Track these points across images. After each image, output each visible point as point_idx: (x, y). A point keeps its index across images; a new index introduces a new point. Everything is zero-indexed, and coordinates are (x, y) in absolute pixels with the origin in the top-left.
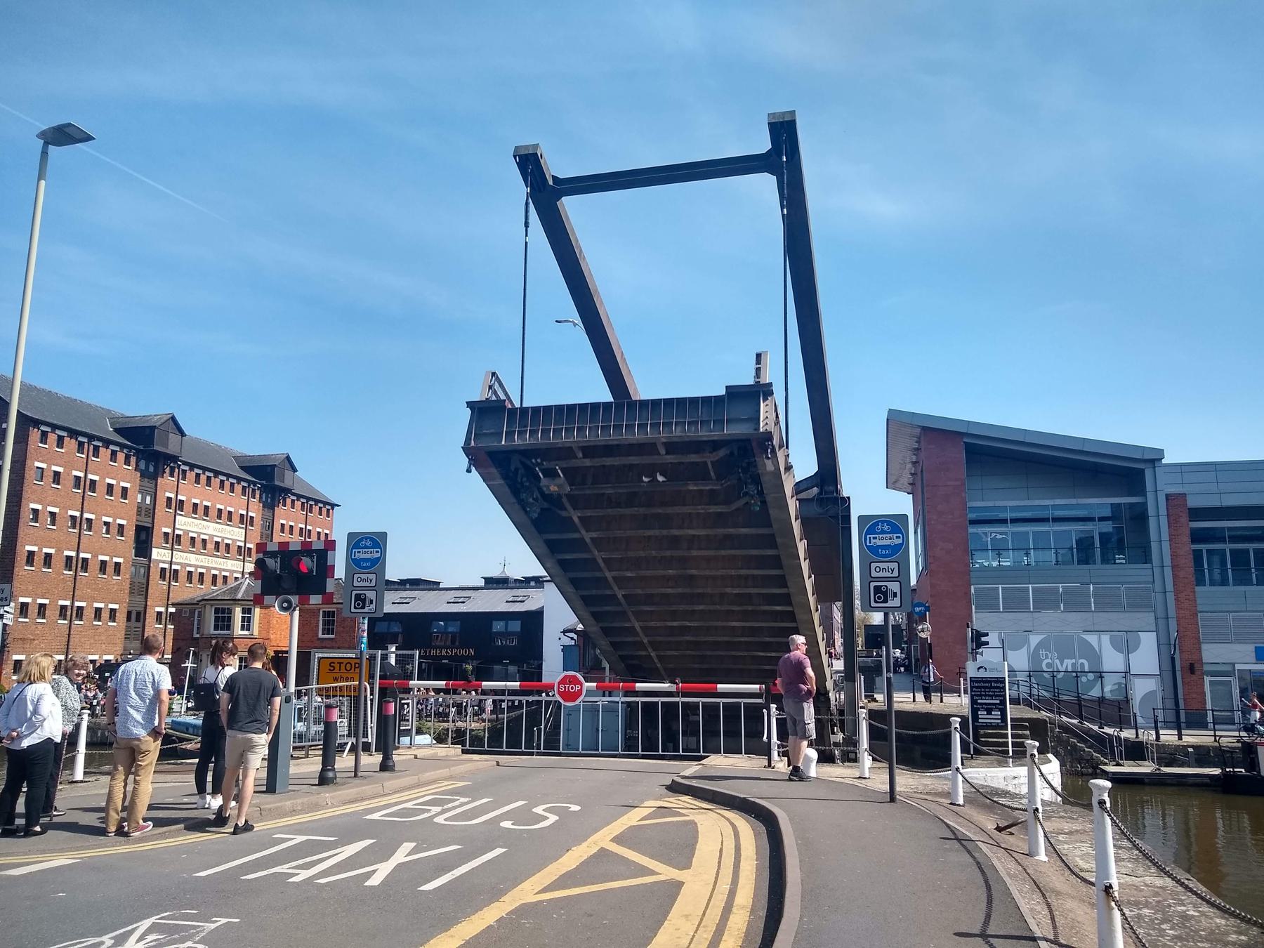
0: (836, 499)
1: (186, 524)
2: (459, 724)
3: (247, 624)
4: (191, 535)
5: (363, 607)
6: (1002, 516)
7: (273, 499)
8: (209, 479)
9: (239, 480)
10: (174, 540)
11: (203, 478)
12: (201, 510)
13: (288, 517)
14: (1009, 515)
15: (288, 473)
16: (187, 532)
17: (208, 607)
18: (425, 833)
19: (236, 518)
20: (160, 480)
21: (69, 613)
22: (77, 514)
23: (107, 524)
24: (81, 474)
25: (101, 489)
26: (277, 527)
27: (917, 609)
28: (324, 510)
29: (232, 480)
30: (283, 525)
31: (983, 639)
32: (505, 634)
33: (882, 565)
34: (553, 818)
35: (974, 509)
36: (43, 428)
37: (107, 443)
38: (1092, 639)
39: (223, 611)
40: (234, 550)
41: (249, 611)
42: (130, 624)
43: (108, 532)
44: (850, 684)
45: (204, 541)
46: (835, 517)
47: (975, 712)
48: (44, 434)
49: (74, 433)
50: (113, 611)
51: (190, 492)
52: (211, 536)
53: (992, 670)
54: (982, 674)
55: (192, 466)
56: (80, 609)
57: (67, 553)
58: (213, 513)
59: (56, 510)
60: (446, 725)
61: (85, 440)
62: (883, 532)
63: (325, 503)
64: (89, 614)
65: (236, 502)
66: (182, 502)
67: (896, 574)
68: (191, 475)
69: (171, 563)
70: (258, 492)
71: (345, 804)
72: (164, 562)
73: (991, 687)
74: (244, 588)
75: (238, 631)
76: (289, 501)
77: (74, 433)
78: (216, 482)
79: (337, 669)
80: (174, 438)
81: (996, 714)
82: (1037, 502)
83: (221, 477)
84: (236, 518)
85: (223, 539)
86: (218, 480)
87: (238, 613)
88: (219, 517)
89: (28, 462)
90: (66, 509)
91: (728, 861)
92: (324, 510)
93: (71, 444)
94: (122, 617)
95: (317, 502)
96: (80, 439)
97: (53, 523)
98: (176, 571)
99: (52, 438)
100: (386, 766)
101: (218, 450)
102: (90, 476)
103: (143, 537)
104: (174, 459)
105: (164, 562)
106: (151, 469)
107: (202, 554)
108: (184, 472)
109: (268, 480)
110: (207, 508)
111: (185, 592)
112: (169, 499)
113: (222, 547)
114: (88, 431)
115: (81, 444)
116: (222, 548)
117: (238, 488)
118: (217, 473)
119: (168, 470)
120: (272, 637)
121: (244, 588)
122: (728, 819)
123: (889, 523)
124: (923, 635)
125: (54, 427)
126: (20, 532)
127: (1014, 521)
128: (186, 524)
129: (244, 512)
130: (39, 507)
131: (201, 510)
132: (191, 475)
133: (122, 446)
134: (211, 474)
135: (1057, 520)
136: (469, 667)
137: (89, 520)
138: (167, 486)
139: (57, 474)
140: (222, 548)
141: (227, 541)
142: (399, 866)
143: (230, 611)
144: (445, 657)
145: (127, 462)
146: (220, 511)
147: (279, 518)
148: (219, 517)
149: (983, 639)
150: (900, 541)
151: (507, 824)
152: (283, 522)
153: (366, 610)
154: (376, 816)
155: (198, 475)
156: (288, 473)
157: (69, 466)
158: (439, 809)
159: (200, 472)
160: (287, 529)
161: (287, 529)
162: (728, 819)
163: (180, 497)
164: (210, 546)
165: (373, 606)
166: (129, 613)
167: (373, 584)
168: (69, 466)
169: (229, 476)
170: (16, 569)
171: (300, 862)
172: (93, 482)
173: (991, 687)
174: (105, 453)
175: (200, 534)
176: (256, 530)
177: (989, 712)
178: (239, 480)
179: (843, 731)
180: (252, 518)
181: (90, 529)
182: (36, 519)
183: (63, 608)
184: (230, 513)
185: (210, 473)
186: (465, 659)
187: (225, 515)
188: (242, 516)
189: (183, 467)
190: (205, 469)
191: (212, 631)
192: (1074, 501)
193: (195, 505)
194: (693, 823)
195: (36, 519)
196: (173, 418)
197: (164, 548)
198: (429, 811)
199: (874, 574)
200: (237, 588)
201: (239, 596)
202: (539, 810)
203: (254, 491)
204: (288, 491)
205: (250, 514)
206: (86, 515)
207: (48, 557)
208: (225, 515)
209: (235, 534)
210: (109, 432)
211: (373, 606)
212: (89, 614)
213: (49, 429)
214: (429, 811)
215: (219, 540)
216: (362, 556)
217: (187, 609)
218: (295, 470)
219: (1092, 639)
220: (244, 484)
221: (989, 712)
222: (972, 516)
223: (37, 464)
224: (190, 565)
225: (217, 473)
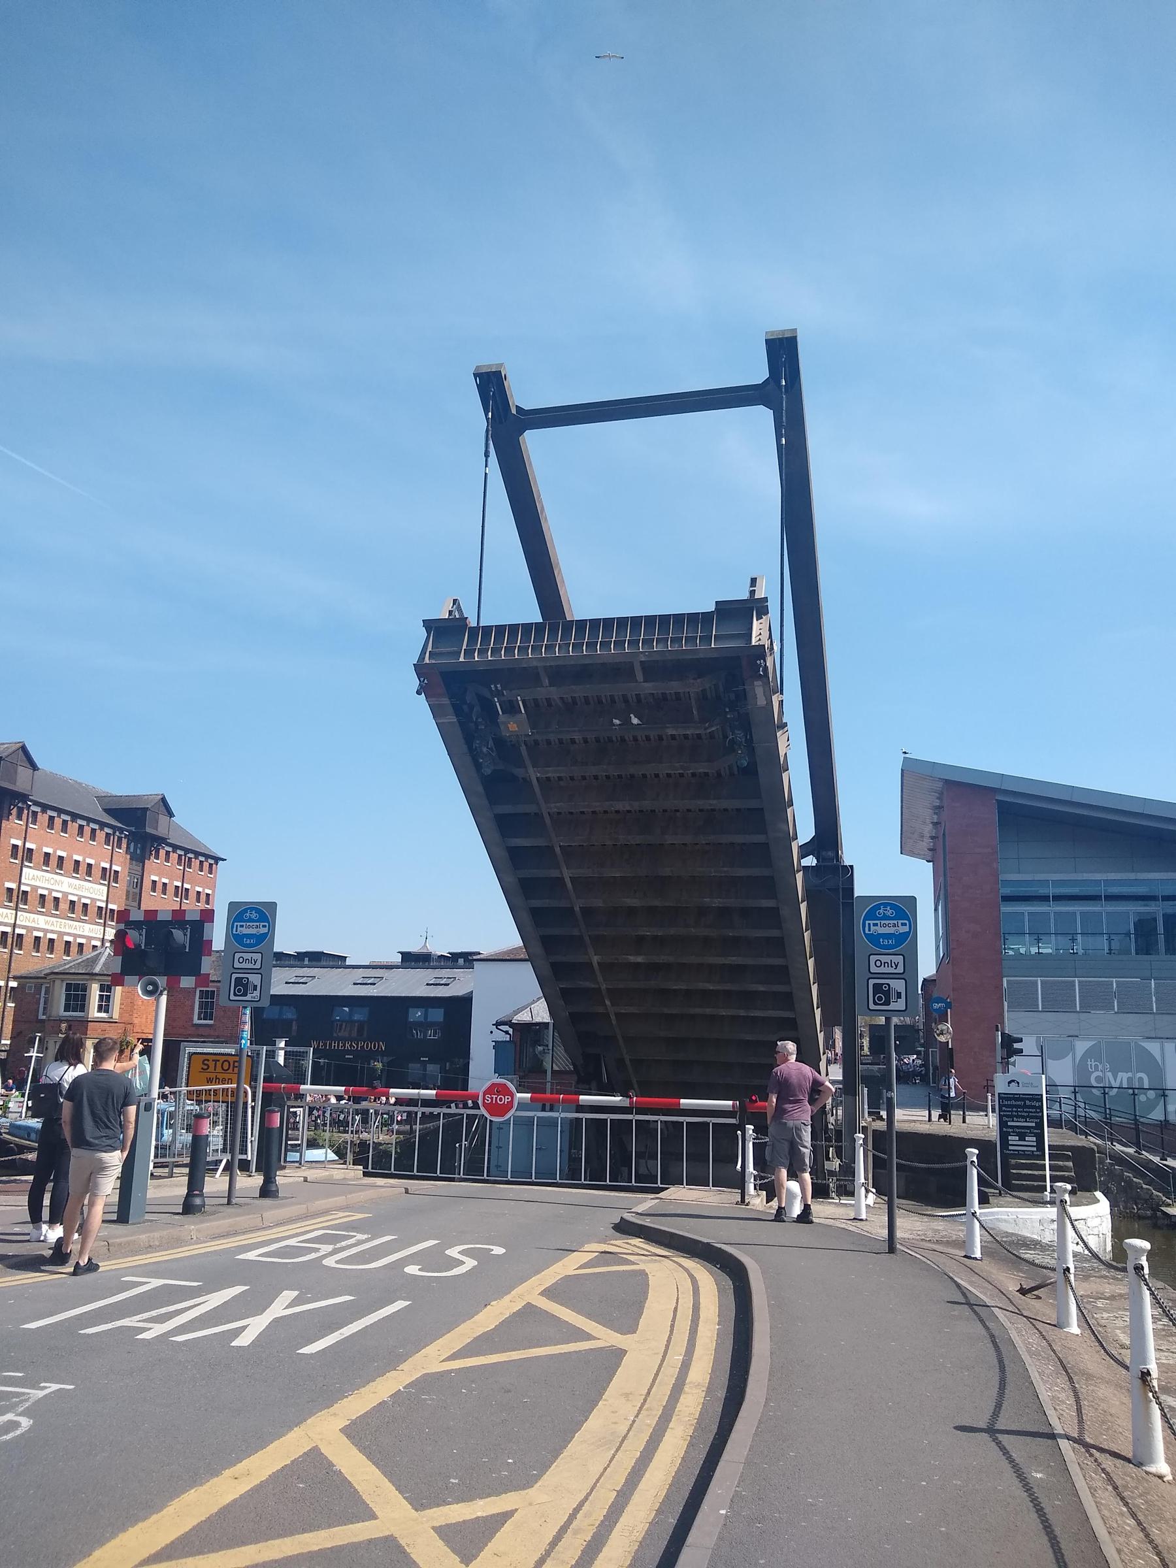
2: (365, 1136)
3: (104, 1006)
4: (41, 891)
5: (245, 994)
6: (1042, 891)
7: (143, 849)
8: (65, 823)
9: (103, 825)
11: (58, 822)
12: (54, 862)
13: (160, 870)
14: (1051, 891)
15: (163, 819)
17: (58, 983)
18: (311, 1279)
19: (97, 873)
20: (4, 823)
26: (147, 885)
27: (936, 1006)
28: (206, 865)
30: (154, 882)
31: (1016, 1046)
32: (424, 1025)
33: (884, 959)
34: (470, 1263)
35: (1007, 883)
38: (1153, 1047)
39: (76, 987)
40: (92, 911)
45: (56, 899)
46: (836, 890)
47: (1004, 1136)
51: (42, 838)
52: (66, 894)
53: (1026, 1085)
54: (1013, 1089)
55: (45, 807)
62: (886, 918)
63: (207, 857)
66: (30, 850)
67: (900, 970)
68: (43, 818)
70: (124, 841)
71: (214, 1238)
72: (6, 925)
73: (1025, 1106)
74: (103, 960)
75: (94, 1013)
76: (162, 853)
78: (73, 827)
79: (211, 1069)
80: (23, 773)
81: (1031, 1140)
82: (1086, 876)
83: (80, 822)
84: (97, 873)
85: (80, 897)
87: (95, 991)
88: (76, 870)
91: (684, 1325)
92: (206, 865)
95: (197, 854)
98: (20, 936)
100: (267, 1191)
101: (77, 788)
104: (24, 798)
105: (6, 925)
108: (35, 814)
109: (137, 827)
110: (61, 858)
111: (30, 962)
112: (15, 847)
113: (78, 908)
116: (77, 909)
117: (101, 835)
118: (75, 816)
119: (14, 812)
120: (136, 1021)
121: (103, 960)
122: (686, 1270)
123: (893, 907)
124: (942, 1039)
127: (1058, 898)
129: (107, 866)
131: (54, 862)
132: (43, 818)
134: (68, 818)
135: (1110, 898)
136: (379, 1065)
140: (77, 909)
141: (84, 901)
142: (276, 1320)
143: (85, 988)
144: (349, 1052)
146: (77, 862)
148: (76, 870)
149: (1016, 1046)
150: (906, 929)
151: (412, 1270)
152: (155, 878)
153: (249, 998)
154: (251, 1255)
155: (51, 819)
156: (163, 819)
158: (330, 1248)
160: (159, 887)
161: (159, 887)
162: (686, 1270)
163: (28, 845)
164: (64, 906)
165: (257, 993)
167: (258, 966)
169: (89, 820)
171: (154, 1313)
173: (1025, 1106)
175: (51, 891)
176: (121, 886)
177: (1022, 1138)
178: (103, 825)
179: (839, 1156)
180: (116, 872)
184: (90, 865)
185: (65, 815)
186: (373, 1055)
187: (83, 868)
188: (104, 869)
191: (62, 1012)
192: (1132, 876)
193: (47, 855)
194: (643, 1274)
196: (24, 749)
197: (7, 907)
198: (318, 1250)
199: (873, 969)
200: (94, 960)
201: (97, 970)
202: (454, 1252)
203: (120, 839)
204: (162, 841)
205: (115, 868)
208: (83, 868)
209: (94, 892)
211: (257, 993)
214: (318, 1250)
215: (75, 898)
216: (245, 931)
217: (31, 983)
218: (171, 815)
219: (1153, 1047)
220: (107, 830)
221: (1022, 1138)
222: (1006, 891)
225: (75, 816)
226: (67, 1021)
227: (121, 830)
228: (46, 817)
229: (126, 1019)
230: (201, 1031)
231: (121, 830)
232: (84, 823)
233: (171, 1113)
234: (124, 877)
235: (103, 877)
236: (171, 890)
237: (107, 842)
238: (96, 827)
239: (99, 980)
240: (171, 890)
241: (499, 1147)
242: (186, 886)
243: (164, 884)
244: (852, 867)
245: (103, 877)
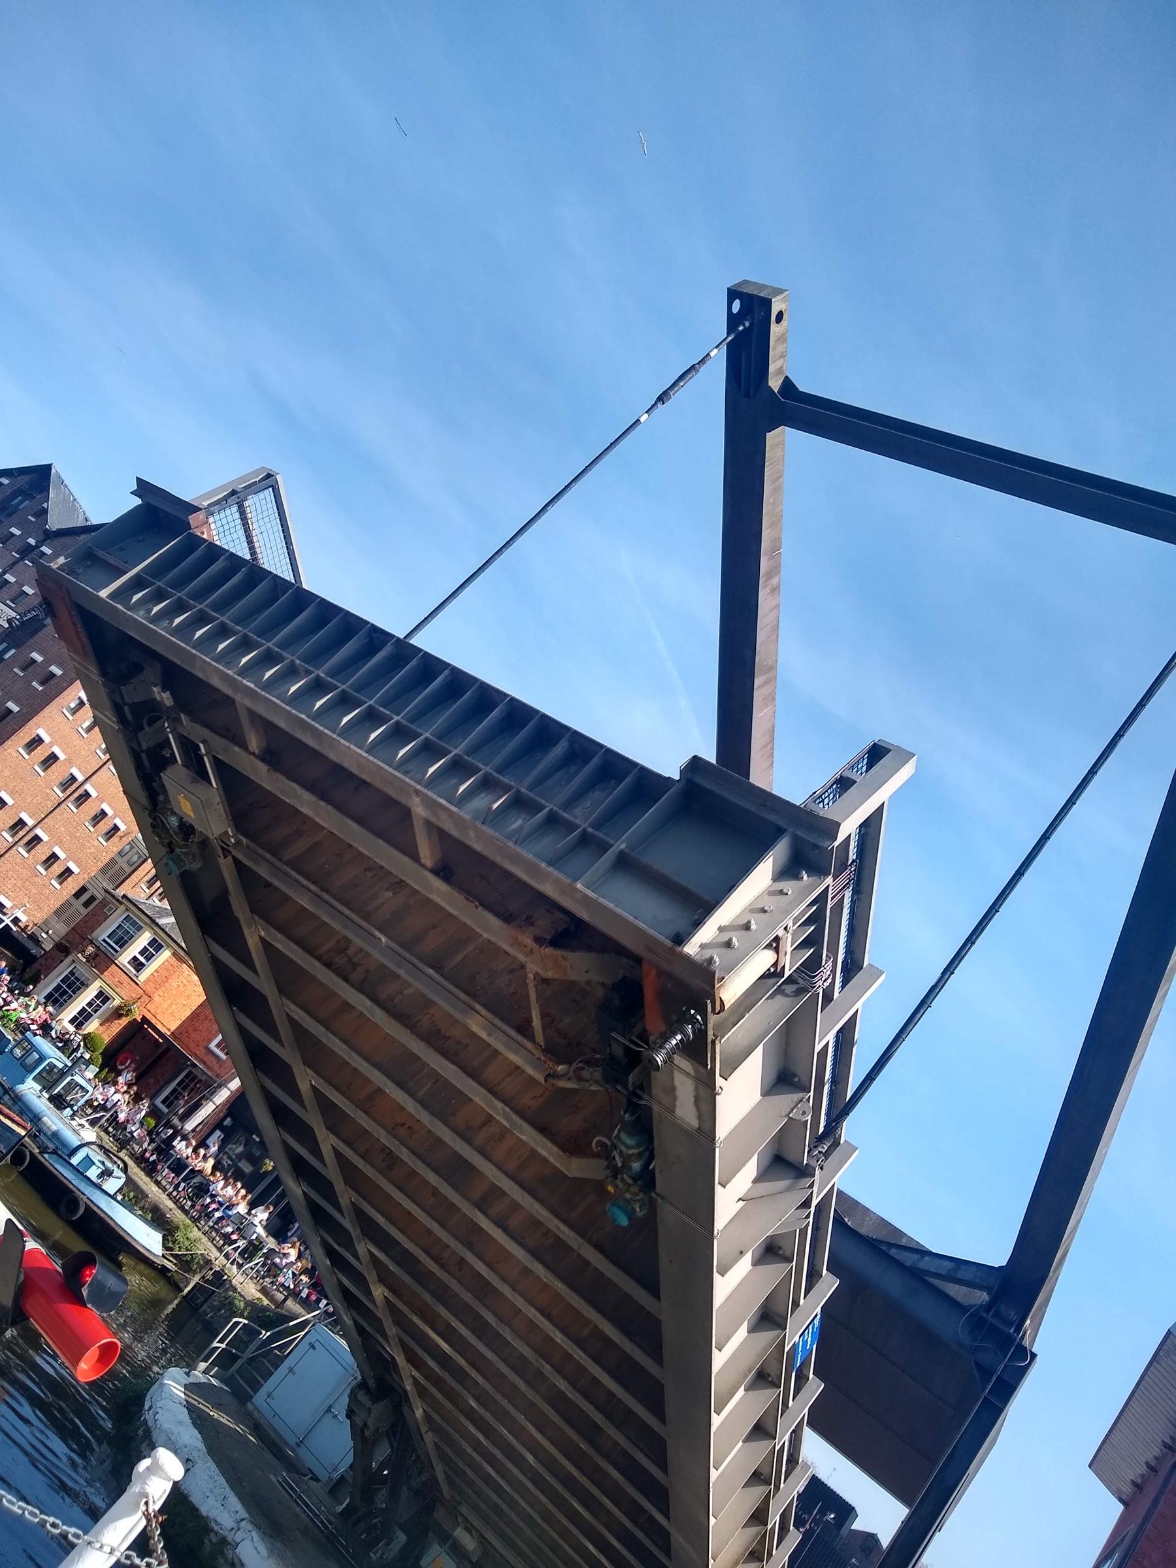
17: (122, 908)
21: (21, 833)
39: (134, 924)
41: (159, 948)
42: (73, 901)
50: (68, 872)
56: (37, 839)
57: (75, 771)
60: (214, 1253)
64: (42, 852)
75: (125, 958)
87: (144, 939)
94: (72, 885)
120: (156, 998)
126: (47, 710)
166: (83, 890)
170: (9, 743)
183: (21, 823)
207: (53, 758)
212: (42, 852)
226: (98, 948)
229: (148, 989)
230: (209, 1059)
233: (52, 1066)
239: (156, 933)
241: (291, 1370)
244: (1034, 1356)
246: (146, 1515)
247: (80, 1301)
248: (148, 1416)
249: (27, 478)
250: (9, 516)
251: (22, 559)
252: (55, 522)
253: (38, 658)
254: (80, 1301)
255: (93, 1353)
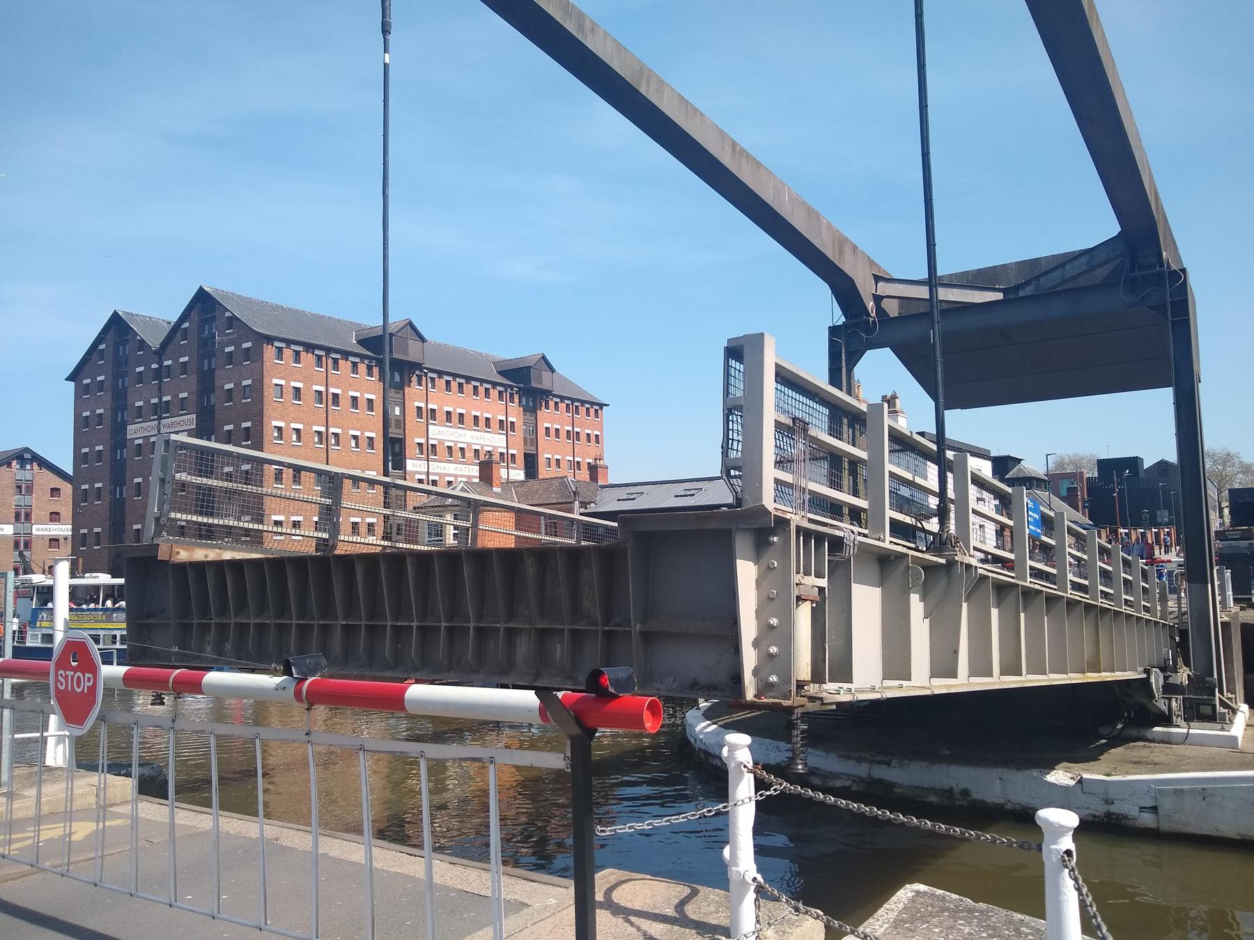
0: (1160, 275)
1: (440, 433)
8: (487, 390)
9: (495, 384)
10: (429, 451)
11: (454, 385)
12: (455, 418)
13: (550, 418)
15: (546, 375)
16: (441, 442)
20: (407, 389)
22: (323, 429)
23: (355, 437)
24: (322, 389)
25: (345, 402)
26: (541, 432)
28: (592, 411)
29: (458, 380)
30: (547, 429)
36: (277, 344)
37: (346, 354)
43: (357, 446)
44: (1196, 586)
45: (462, 449)
48: (280, 350)
49: (310, 347)
51: (441, 399)
52: (469, 445)
55: (441, 374)
58: (469, 420)
59: (299, 426)
61: (323, 353)
63: (592, 404)
65: (493, 408)
66: (433, 411)
68: (441, 383)
69: (428, 474)
70: (376, 370)
72: (420, 473)
76: (551, 404)
77: (310, 347)
78: (468, 388)
80: (414, 345)
86: (471, 387)
89: (266, 380)
90: (310, 424)
92: (592, 411)
93: (308, 358)
95: (583, 402)
96: (317, 352)
97: (299, 439)
99: (288, 353)
101: (478, 357)
102: (332, 390)
103: (397, 449)
104: (419, 366)
105: (420, 473)
106: (397, 378)
107: (461, 463)
108: (433, 379)
109: (526, 384)
110: (461, 415)
112: (419, 409)
114: (326, 344)
115: (319, 358)
118: (469, 379)
119: (414, 379)
125: (289, 342)
128: (440, 433)
129: (503, 418)
130: (281, 424)
132: (441, 383)
133: (362, 357)
134: (463, 381)
137: (336, 435)
138: (416, 395)
139: (297, 390)
145: (370, 374)
146: (476, 418)
147: (543, 422)
155: (475, 388)
156: (546, 375)
157: (309, 380)
159: (450, 378)
160: (552, 432)
161: (552, 432)
163: (430, 406)
168: (309, 380)
169: (482, 381)
172: (336, 396)
174: (345, 365)
175: (456, 443)
176: (518, 435)
178: (495, 384)
179: (1187, 664)
180: (512, 423)
181: (337, 444)
182: (280, 437)
184: (488, 419)
185: (462, 378)
189: (430, 375)
190: (455, 376)
193: (448, 413)
195: (280, 437)
196: (411, 324)
197: (419, 459)
203: (512, 395)
204: (547, 394)
205: (510, 419)
206: (332, 430)
210: (352, 344)
213: (283, 345)
218: (552, 370)
220: (500, 388)
223: (275, 381)
224: (449, 475)
225: (469, 379)
227: (511, 387)
228: (443, 382)
231: (511, 387)
232: (477, 384)
234: (520, 426)
235: (501, 427)
236: (563, 434)
237: (501, 398)
238: (489, 386)
240: (563, 434)
242: (577, 430)
243: (557, 430)
245: (501, 427)
246: (750, 771)
247: (615, 697)
248: (698, 745)
249: (110, 335)
250: (126, 364)
251: (161, 381)
252: (154, 343)
253: (230, 427)
254: (615, 697)
255: (647, 715)
